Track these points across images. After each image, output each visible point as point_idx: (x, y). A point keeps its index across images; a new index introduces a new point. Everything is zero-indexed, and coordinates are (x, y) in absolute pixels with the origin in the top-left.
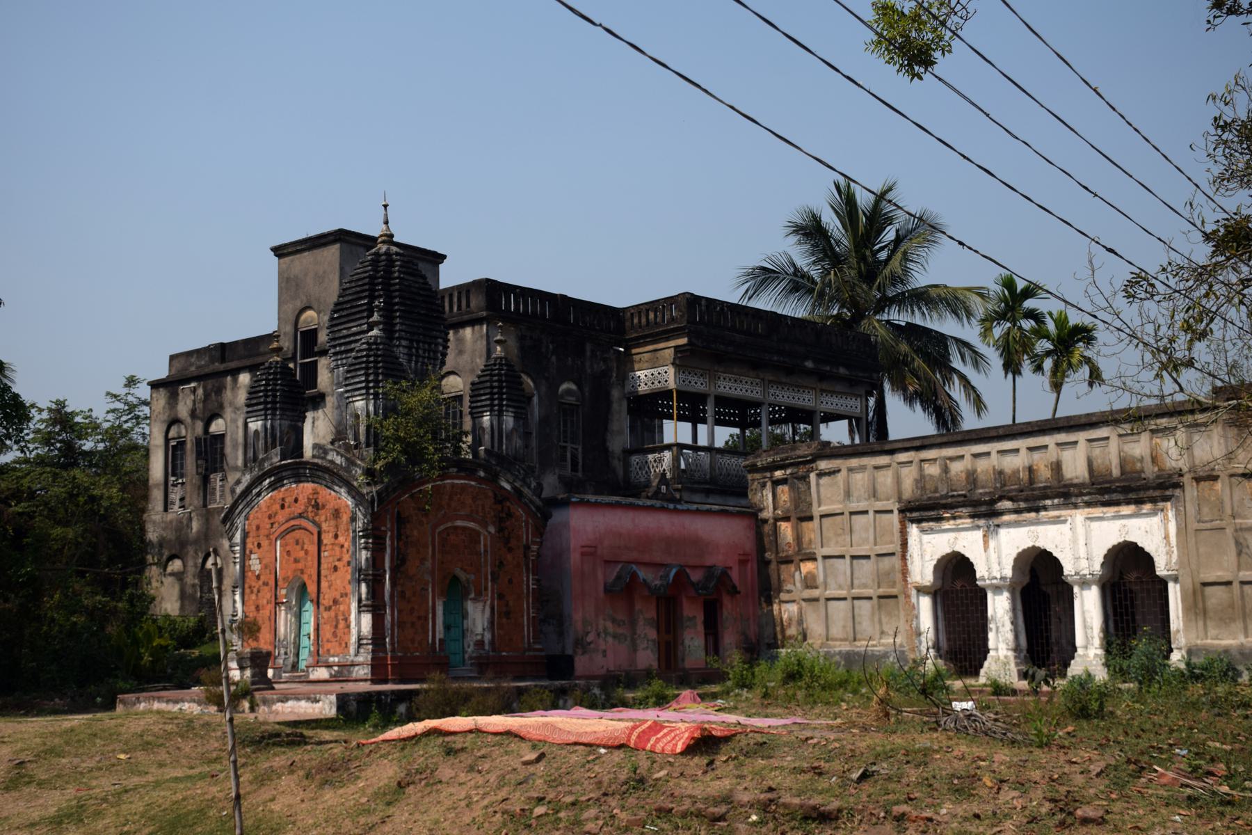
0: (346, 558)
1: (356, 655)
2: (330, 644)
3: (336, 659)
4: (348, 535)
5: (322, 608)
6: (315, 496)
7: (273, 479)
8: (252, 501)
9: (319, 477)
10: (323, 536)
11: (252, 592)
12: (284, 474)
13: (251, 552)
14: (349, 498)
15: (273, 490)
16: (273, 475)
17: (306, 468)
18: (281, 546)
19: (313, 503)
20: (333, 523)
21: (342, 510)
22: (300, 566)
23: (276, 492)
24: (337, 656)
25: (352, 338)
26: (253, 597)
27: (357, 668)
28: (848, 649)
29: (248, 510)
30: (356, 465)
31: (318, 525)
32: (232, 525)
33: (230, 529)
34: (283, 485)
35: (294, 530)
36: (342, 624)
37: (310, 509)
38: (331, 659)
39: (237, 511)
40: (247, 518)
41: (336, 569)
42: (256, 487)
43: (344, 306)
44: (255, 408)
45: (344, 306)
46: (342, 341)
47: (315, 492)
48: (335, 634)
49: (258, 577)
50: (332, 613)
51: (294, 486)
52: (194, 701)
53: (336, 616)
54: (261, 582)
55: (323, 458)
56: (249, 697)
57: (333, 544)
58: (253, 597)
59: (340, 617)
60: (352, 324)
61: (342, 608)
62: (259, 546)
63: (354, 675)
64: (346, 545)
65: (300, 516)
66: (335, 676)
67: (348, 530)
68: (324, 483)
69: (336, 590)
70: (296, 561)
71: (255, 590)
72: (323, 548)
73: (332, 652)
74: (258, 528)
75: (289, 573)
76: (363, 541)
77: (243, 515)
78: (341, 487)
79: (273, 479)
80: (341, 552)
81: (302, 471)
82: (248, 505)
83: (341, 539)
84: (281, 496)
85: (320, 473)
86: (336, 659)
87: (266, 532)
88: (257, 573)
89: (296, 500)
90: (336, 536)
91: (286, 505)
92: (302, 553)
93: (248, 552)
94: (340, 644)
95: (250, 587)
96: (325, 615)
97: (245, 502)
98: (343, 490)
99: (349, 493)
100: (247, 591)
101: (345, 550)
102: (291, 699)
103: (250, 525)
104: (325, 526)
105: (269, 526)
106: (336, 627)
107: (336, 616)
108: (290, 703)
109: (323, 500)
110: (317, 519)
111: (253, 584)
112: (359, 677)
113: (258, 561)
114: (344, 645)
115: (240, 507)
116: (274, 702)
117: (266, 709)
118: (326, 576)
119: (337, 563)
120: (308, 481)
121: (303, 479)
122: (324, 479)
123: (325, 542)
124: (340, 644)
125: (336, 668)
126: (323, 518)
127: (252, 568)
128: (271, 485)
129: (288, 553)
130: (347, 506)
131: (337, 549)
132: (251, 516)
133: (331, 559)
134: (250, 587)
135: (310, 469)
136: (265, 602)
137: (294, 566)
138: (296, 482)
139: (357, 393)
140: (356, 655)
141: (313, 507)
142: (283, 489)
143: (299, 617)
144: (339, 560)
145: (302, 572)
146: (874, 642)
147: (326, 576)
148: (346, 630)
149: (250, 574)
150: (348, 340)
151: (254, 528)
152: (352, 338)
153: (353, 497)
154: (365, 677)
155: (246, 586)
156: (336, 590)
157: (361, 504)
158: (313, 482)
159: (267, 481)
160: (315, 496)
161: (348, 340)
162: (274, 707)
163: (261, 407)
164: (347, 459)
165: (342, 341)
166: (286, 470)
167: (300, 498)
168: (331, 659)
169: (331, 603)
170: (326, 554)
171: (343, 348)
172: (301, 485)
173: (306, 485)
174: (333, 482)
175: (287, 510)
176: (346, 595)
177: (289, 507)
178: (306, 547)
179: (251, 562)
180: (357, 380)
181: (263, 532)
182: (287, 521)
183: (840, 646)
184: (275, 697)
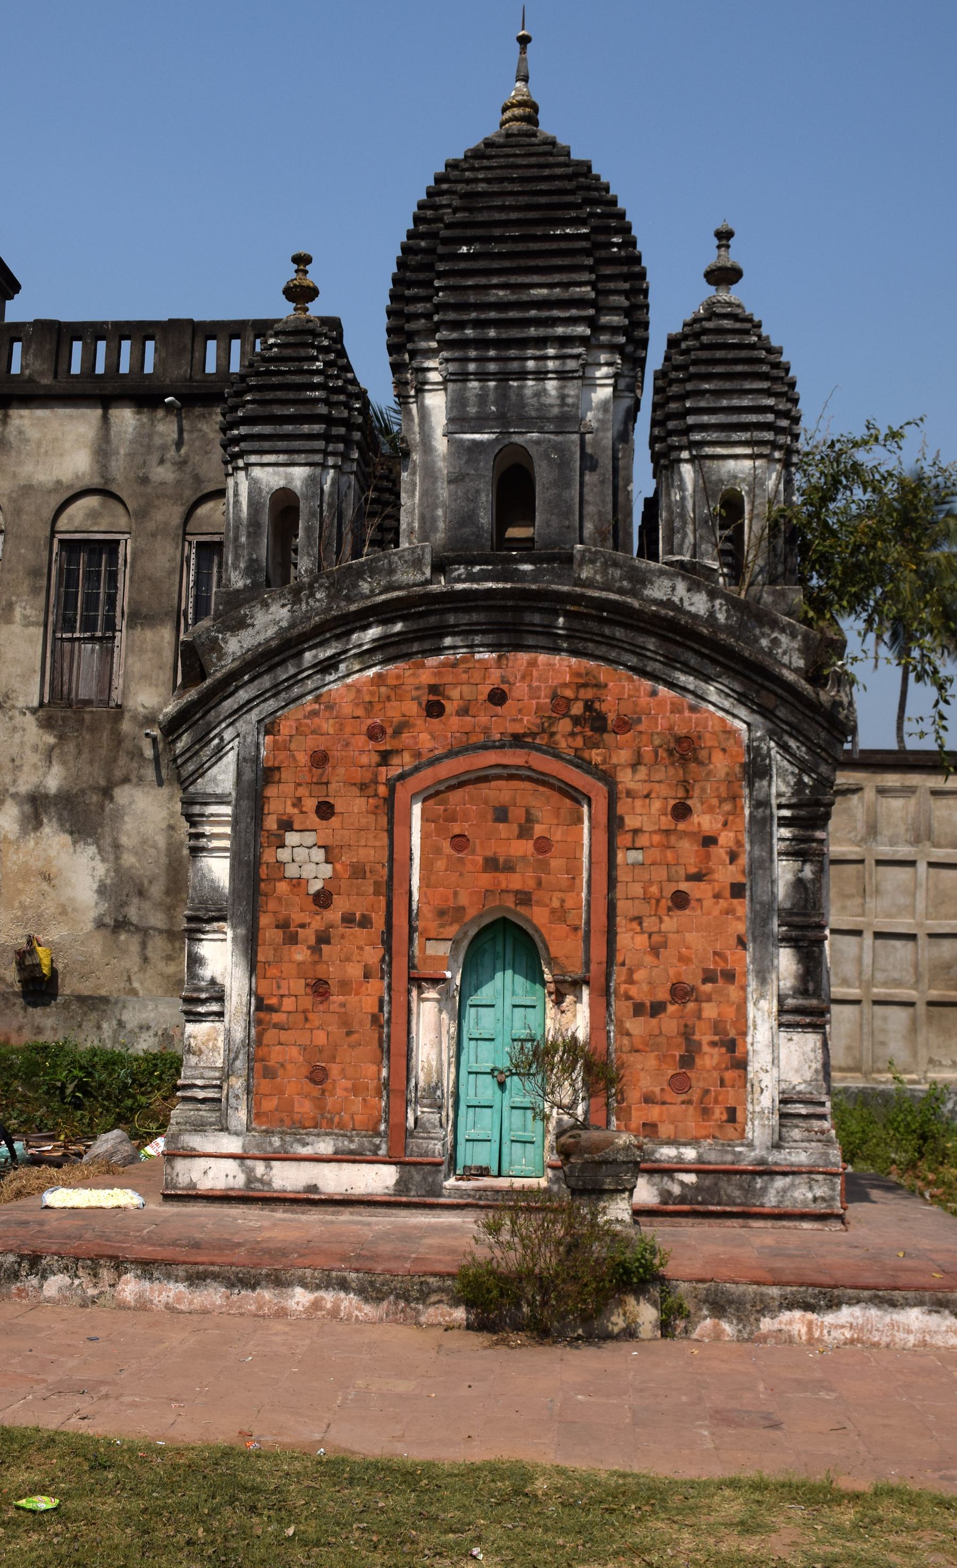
0: (726, 874)
1: (777, 1146)
2: (654, 1113)
3: (690, 1154)
4: (736, 811)
5: (619, 1007)
6: (588, 694)
7: (399, 627)
8: (294, 680)
9: (611, 642)
10: (621, 809)
11: (292, 939)
12: (452, 619)
13: (287, 825)
14: (742, 712)
15: (384, 662)
16: (403, 618)
17: (556, 614)
18: (425, 819)
19: (577, 709)
20: (667, 773)
21: (708, 741)
22: (515, 881)
23: (401, 665)
24: (693, 1142)
25: (533, 313)
26: (300, 954)
27: (780, 1183)
28: (861, 1085)
29: (272, 704)
30: (774, 624)
31: (608, 778)
32: (202, 740)
33: (192, 752)
34: (438, 651)
35: (486, 779)
36: (710, 1058)
37: (565, 726)
38: (667, 1152)
39: (229, 705)
40: (269, 727)
41: (680, 901)
42: (323, 644)
43: (497, 232)
44: (289, 428)
45: (497, 232)
46: (493, 315)
47: (585, 682)
48: (680, 1084)
49: (323, 899)
50: (669, 1023)
51: (486, 656)
52: (343, 1285)
53: (687, 1033)
54: (333, 915)
55: (634, 593)
56: (655, 1292)
57: (667, 832)
58: (300, 954)
59: (704, 1037)
60: (536, 279)
61: (710, 1011)
62: (325, 810)
63: (771, 1201)
64: (726, 839)
65: (517, 741)
66: (682, 1199)
67: (734, 798)
68: (633, 660)
69: (684, 959)
70: (492, 864)
71: (308, 935)
72: (623, 839)
73: (665, 1130)
74: (320, 759)
75: (463, 900)
76: (785, 832)
77: (254, 716)
78: (708, 679)
79: (399, 627)
80: (708, 857)
81: (537, 618)
82: (276, 690)
83: (704, 821)
84: (426, 677)
85: (619, 633)
86: (690, 1154)
87: (359, 775)
88: (315, 886)
89: (498, 697)
90: (682, 811)
91: (450, 707)
92: (527, 847)
93: (271, 823)
94: (706, 1112)
95: (283, 925)
96: (636, 1026)
97: (266, 681)
98: (711, 691)
99: (742, 699)
100: (270, 934)
101: (720, 852)
102: (854, 1301)
103: (276, 747)
104: (626, 779)
105: (376, 758)
106: (687, 1061)
107: (687, 1033)
108: (846, 1314)
109: (626, 708)
110: (596, 756)
111: (297, 917)
112: (788, 1206)
113: (319, 855)
114: (719, 1114)
115: (243, 695)
116: (764, 1308)
117: (728, 1328)
118: (639, 920)
119: (684, 886)
120: (556, 650)
121: (531, 641)
122: (637, 651)
123: (631, 822)
124: (706, 1112)
125: (690, 1178)
126: (623, 756)
127: (291, 871)
128: (380, 645)
129: (460, 842)
130: (731, 733)
131: (688, 849)
132: (286, 728)
133: (660, 873)
134: (283, 925)
135: (567, 614)
136: (354, 971)
137: (486, 880)
138: (492, 647)
139: (744, 436)
140: (777, 1146)
141: (576, 720)
142: (432, 661)
143: (459, 1017)
144: (697, 877)
145: (524, 898)
146: (914, 1077)
147: (639, 920)
148: (729, 1075)
149: (282, 887)
150: (512, 314)
151: (303, 758)
152: (533, 313)
153: (764, 712)
154: (821, 1208)
155: (264, 920)
156: (684, 959)
157: (796, 733)
158: (574, 652)
159: (374, 632)
160: (588, 694)
161: (512, 314)
162: (767, 1324)
163: (318, 428)
164: (733, 603)
165: (493, 315)
166: (456, 610)
167: (520, 690)
168: (667, 1152)
169: (662, 995)
170: (634, 856)
171: (492, 333)
172: (523, 657)
173: (542, 658)
174: (671, 662)
175: (453, 723)
176: (730, 976)
177: (464, 711)
178: (539, 830)
179: (284, 855)
180: (746, 402)
181: (338, 775)
182: (452, 754)
183: (843, 1079)
184: (774, 1291)
